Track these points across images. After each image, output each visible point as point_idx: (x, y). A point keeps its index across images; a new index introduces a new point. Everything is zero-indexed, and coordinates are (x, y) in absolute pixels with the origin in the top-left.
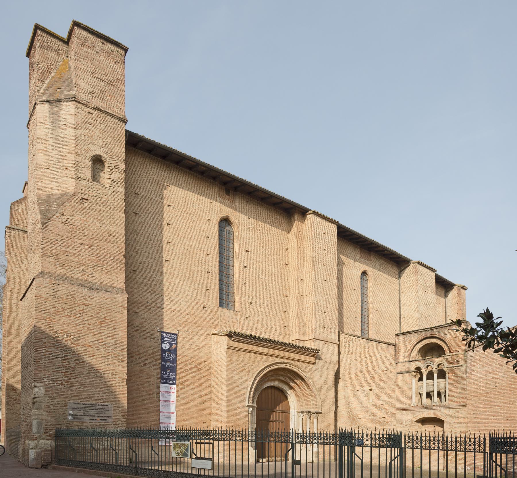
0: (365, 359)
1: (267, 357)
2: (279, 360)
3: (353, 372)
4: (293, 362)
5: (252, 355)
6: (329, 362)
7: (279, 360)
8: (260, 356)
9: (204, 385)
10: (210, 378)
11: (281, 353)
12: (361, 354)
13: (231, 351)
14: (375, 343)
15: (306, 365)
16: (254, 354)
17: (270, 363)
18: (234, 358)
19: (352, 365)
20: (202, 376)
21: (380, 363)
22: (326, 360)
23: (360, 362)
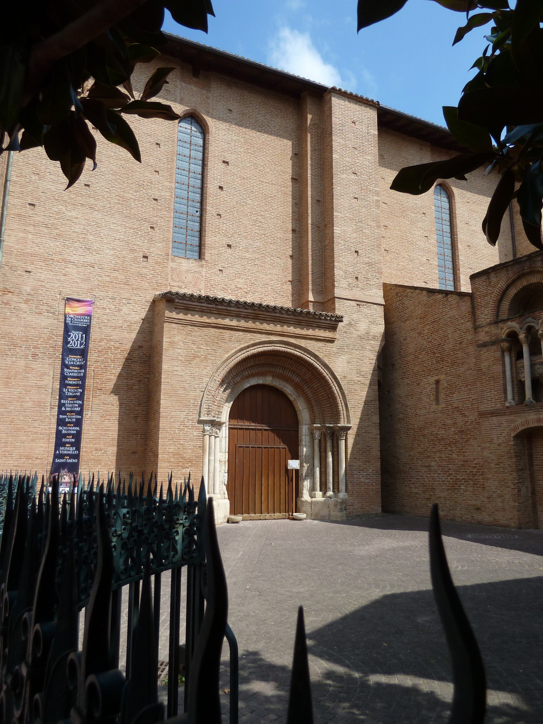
0: (428, 327)
1: (241, 333)
2: (264, 338)
3: (410, 351)
4: (292, 340)
5: (213, 330)
6: (366, 337)
7: (264, 338)
8: (229, 332)
9: (137, 387)
10: (148, 376)
11: (266, 326)
12: (421, 318)
13: (174, 325)
14: (440, 296)
15: (320, 344)
16: (217, 330)
17: (246, 345)
18: (176, 339)
19: (409, 339)
20: (134, 373)
21: (450, 330)
22: (359, 333)
23: (420, 333)
